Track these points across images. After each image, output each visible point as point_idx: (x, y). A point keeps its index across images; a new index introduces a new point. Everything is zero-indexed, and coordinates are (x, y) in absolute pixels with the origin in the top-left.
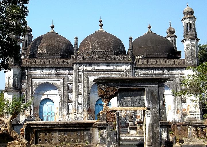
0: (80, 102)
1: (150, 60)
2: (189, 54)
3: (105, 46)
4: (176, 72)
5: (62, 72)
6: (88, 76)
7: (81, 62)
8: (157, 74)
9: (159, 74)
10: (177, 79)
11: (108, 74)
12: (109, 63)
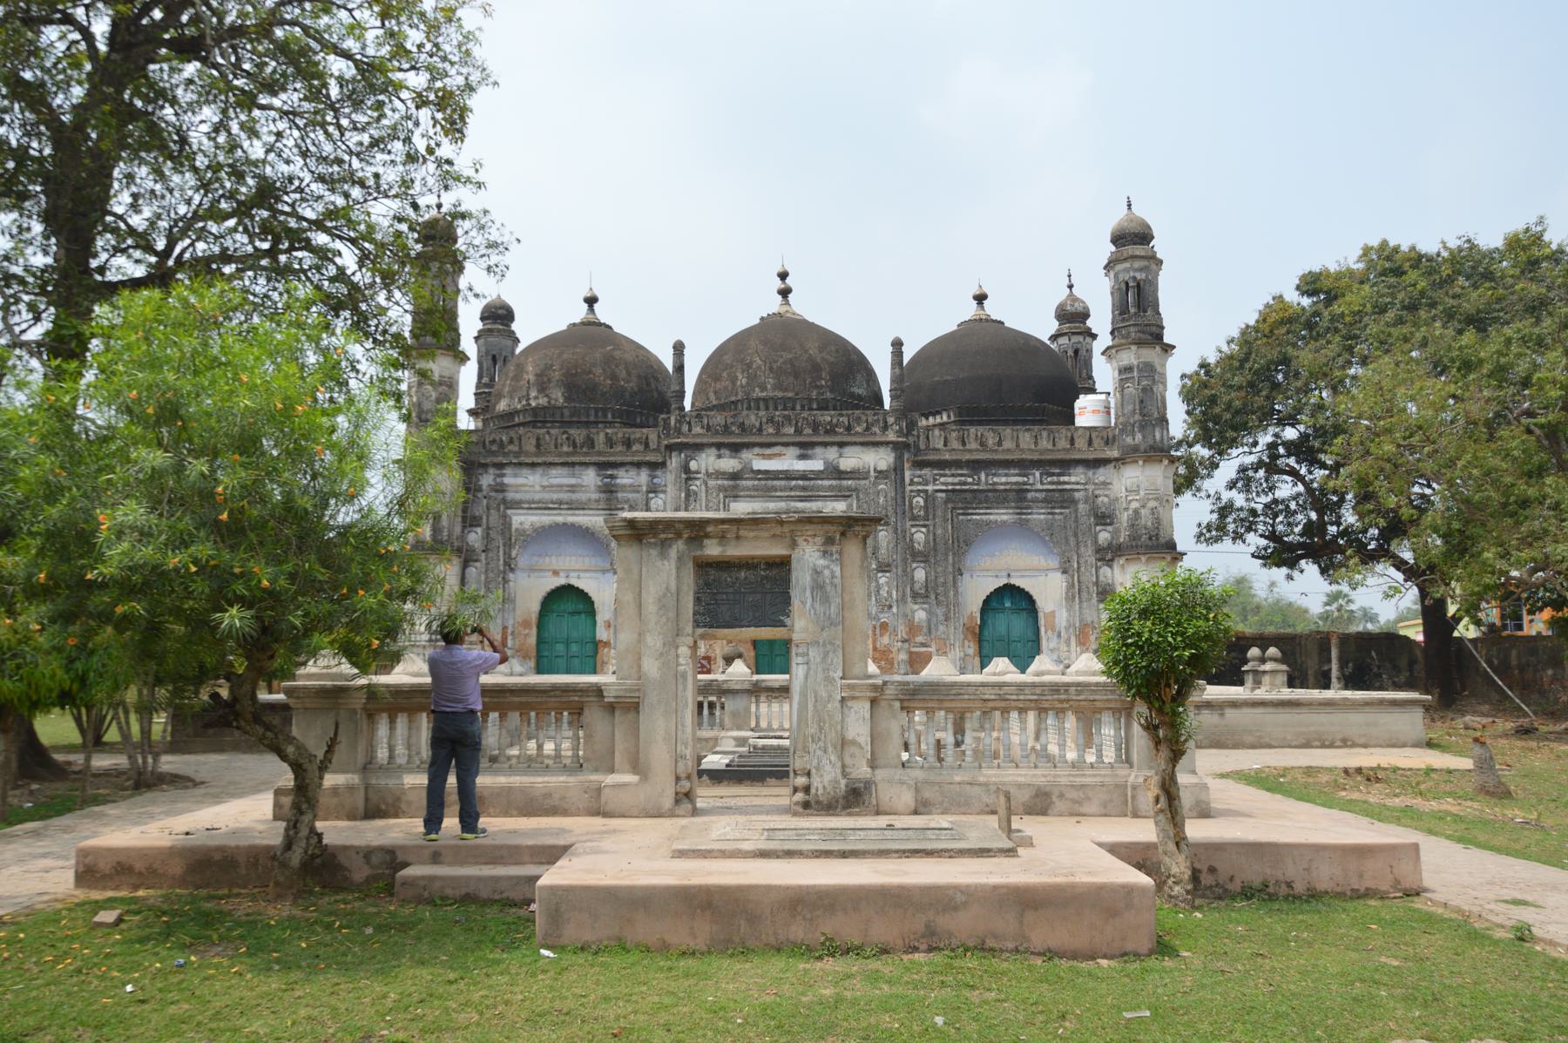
1: (973, 430)
2: (1130, 407)
3: (796, 378)
4: (1077, 477)
5: (625, 478)
7: (698, 440)
10: (1081, 506)
11: (804, 489)
12: (813, 445)
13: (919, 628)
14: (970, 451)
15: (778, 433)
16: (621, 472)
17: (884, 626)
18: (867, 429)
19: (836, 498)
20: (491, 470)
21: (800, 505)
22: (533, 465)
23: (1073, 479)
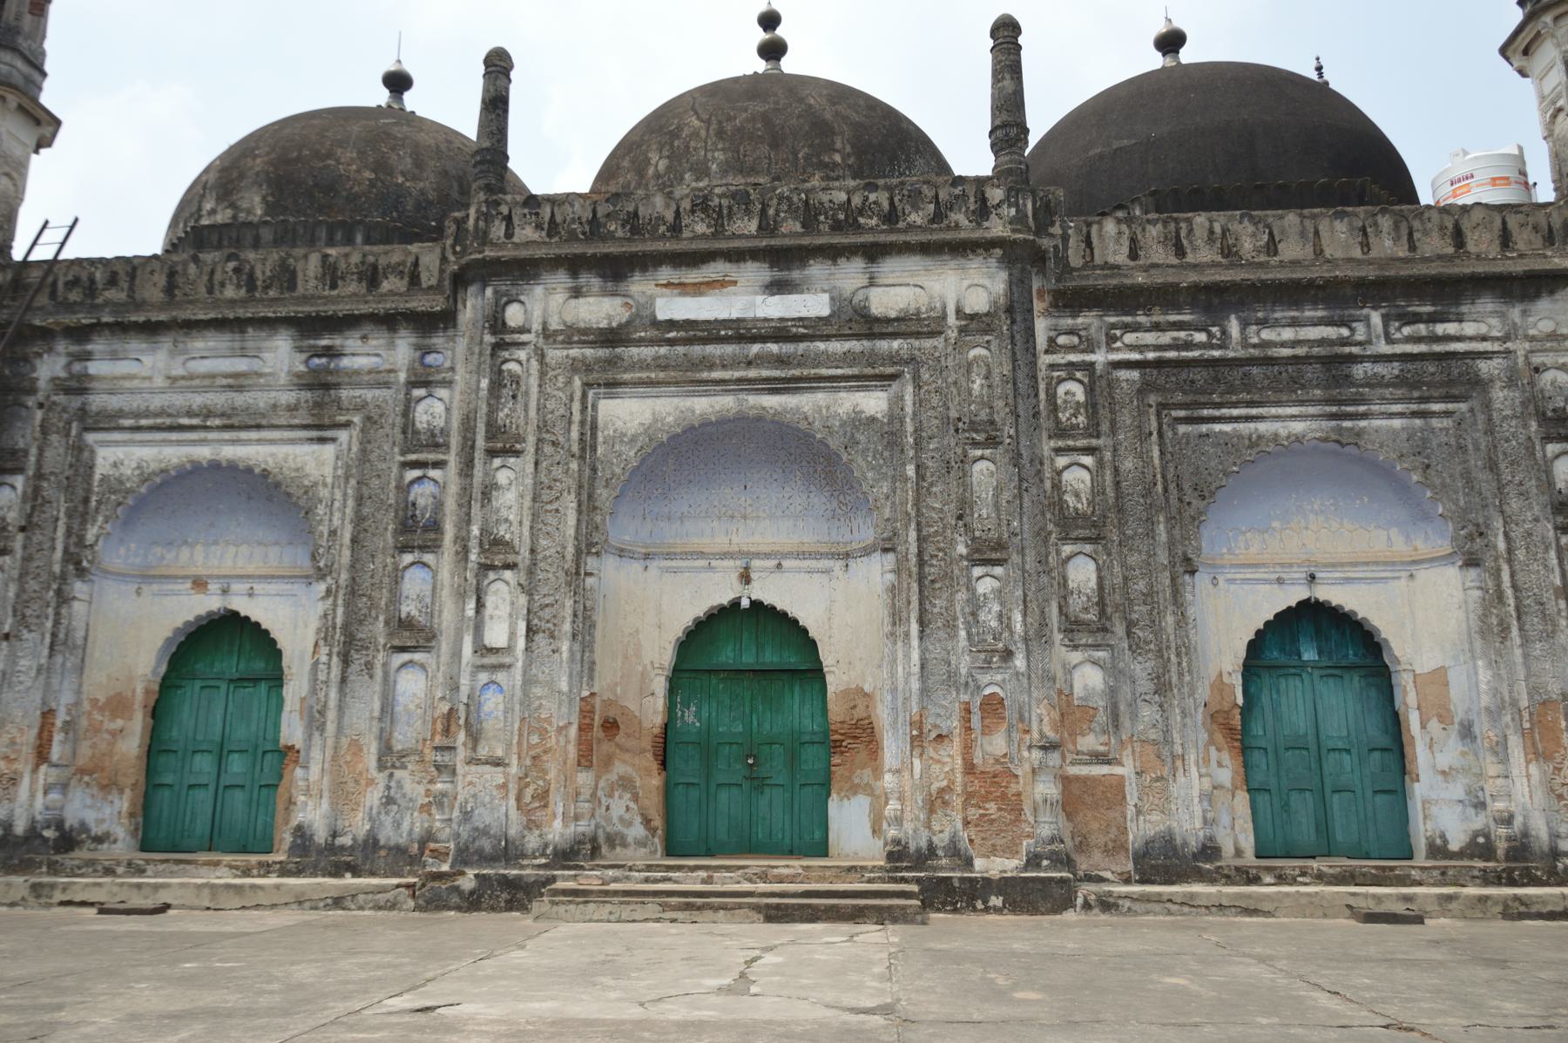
0: (496, 635)
1: (1200, 219)
3: (775, 145)
4: (1476, 325)
5: (363, 354)
6: (587, 385)
8: (1286, 352)
9: (1301, 351)
10: (1499, 395)
11: (781, 361)
13: (1088, 712)
14: (1194, 267)
15: (718, 234)
16: (350, 342)
17: (993, 706)
18: (938, 217)
19: (862, 381)
20: (62, 346)
21: (771, 402)
22: (151, 329)
23: (1469, 329)
